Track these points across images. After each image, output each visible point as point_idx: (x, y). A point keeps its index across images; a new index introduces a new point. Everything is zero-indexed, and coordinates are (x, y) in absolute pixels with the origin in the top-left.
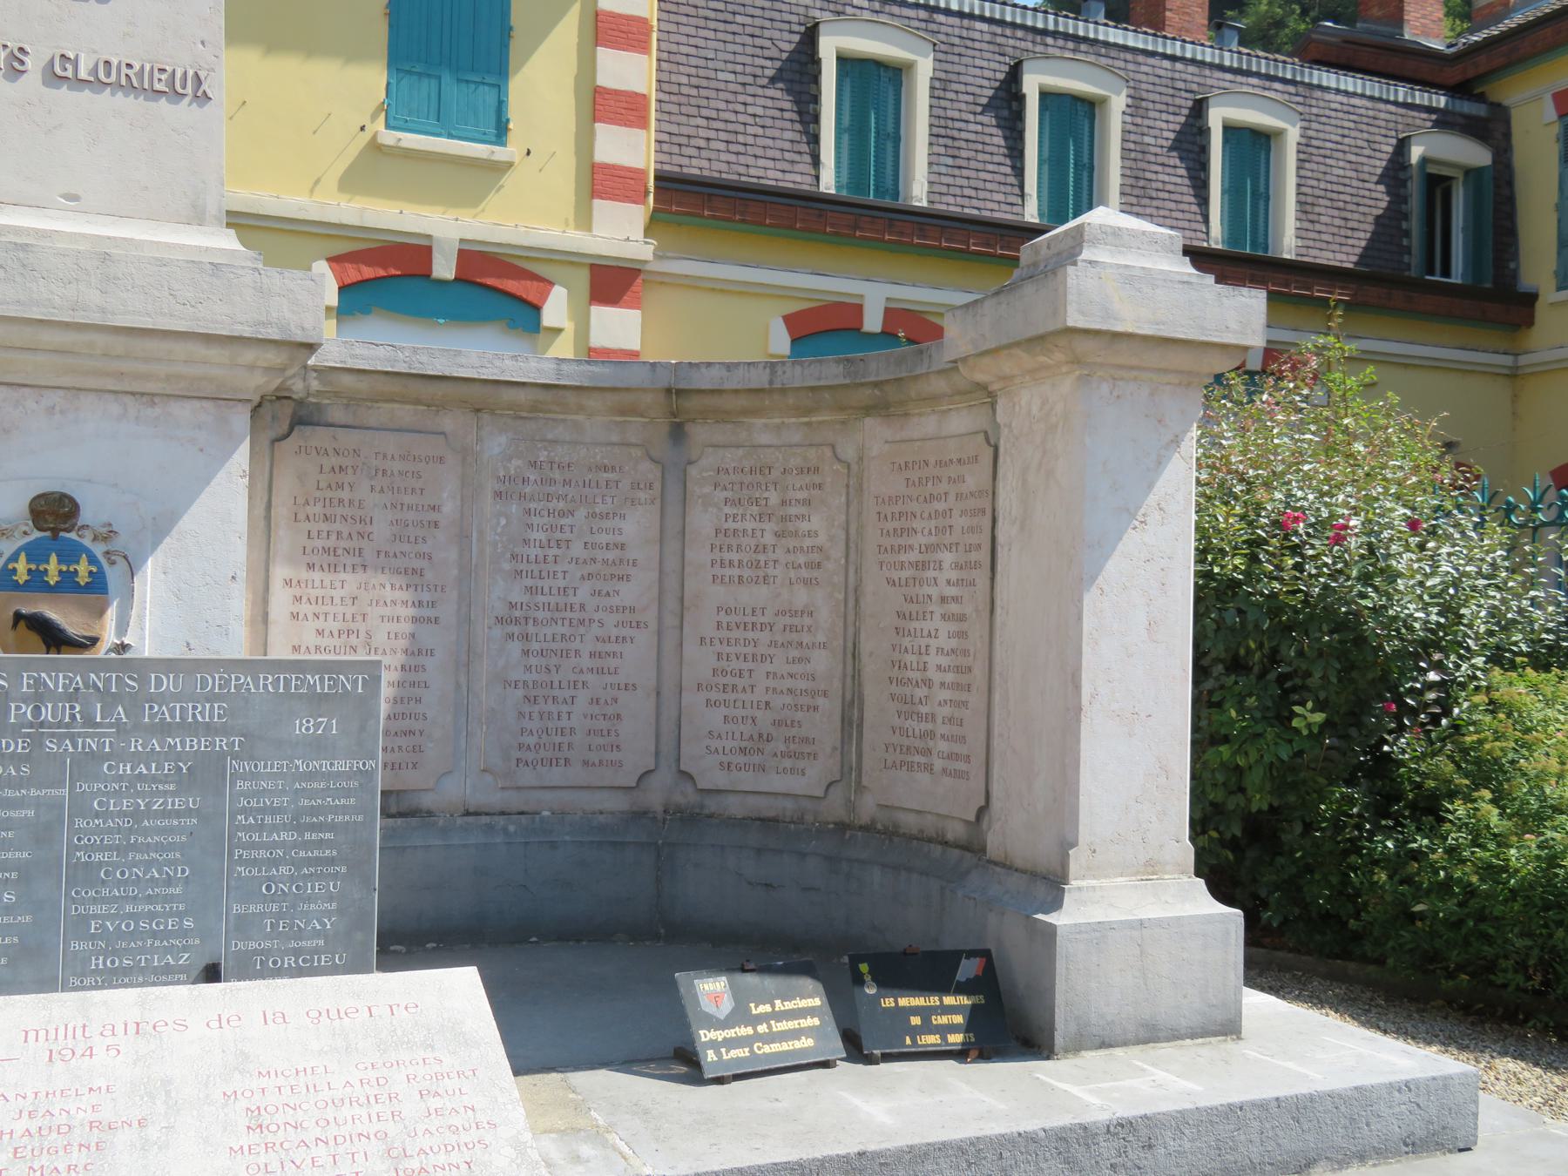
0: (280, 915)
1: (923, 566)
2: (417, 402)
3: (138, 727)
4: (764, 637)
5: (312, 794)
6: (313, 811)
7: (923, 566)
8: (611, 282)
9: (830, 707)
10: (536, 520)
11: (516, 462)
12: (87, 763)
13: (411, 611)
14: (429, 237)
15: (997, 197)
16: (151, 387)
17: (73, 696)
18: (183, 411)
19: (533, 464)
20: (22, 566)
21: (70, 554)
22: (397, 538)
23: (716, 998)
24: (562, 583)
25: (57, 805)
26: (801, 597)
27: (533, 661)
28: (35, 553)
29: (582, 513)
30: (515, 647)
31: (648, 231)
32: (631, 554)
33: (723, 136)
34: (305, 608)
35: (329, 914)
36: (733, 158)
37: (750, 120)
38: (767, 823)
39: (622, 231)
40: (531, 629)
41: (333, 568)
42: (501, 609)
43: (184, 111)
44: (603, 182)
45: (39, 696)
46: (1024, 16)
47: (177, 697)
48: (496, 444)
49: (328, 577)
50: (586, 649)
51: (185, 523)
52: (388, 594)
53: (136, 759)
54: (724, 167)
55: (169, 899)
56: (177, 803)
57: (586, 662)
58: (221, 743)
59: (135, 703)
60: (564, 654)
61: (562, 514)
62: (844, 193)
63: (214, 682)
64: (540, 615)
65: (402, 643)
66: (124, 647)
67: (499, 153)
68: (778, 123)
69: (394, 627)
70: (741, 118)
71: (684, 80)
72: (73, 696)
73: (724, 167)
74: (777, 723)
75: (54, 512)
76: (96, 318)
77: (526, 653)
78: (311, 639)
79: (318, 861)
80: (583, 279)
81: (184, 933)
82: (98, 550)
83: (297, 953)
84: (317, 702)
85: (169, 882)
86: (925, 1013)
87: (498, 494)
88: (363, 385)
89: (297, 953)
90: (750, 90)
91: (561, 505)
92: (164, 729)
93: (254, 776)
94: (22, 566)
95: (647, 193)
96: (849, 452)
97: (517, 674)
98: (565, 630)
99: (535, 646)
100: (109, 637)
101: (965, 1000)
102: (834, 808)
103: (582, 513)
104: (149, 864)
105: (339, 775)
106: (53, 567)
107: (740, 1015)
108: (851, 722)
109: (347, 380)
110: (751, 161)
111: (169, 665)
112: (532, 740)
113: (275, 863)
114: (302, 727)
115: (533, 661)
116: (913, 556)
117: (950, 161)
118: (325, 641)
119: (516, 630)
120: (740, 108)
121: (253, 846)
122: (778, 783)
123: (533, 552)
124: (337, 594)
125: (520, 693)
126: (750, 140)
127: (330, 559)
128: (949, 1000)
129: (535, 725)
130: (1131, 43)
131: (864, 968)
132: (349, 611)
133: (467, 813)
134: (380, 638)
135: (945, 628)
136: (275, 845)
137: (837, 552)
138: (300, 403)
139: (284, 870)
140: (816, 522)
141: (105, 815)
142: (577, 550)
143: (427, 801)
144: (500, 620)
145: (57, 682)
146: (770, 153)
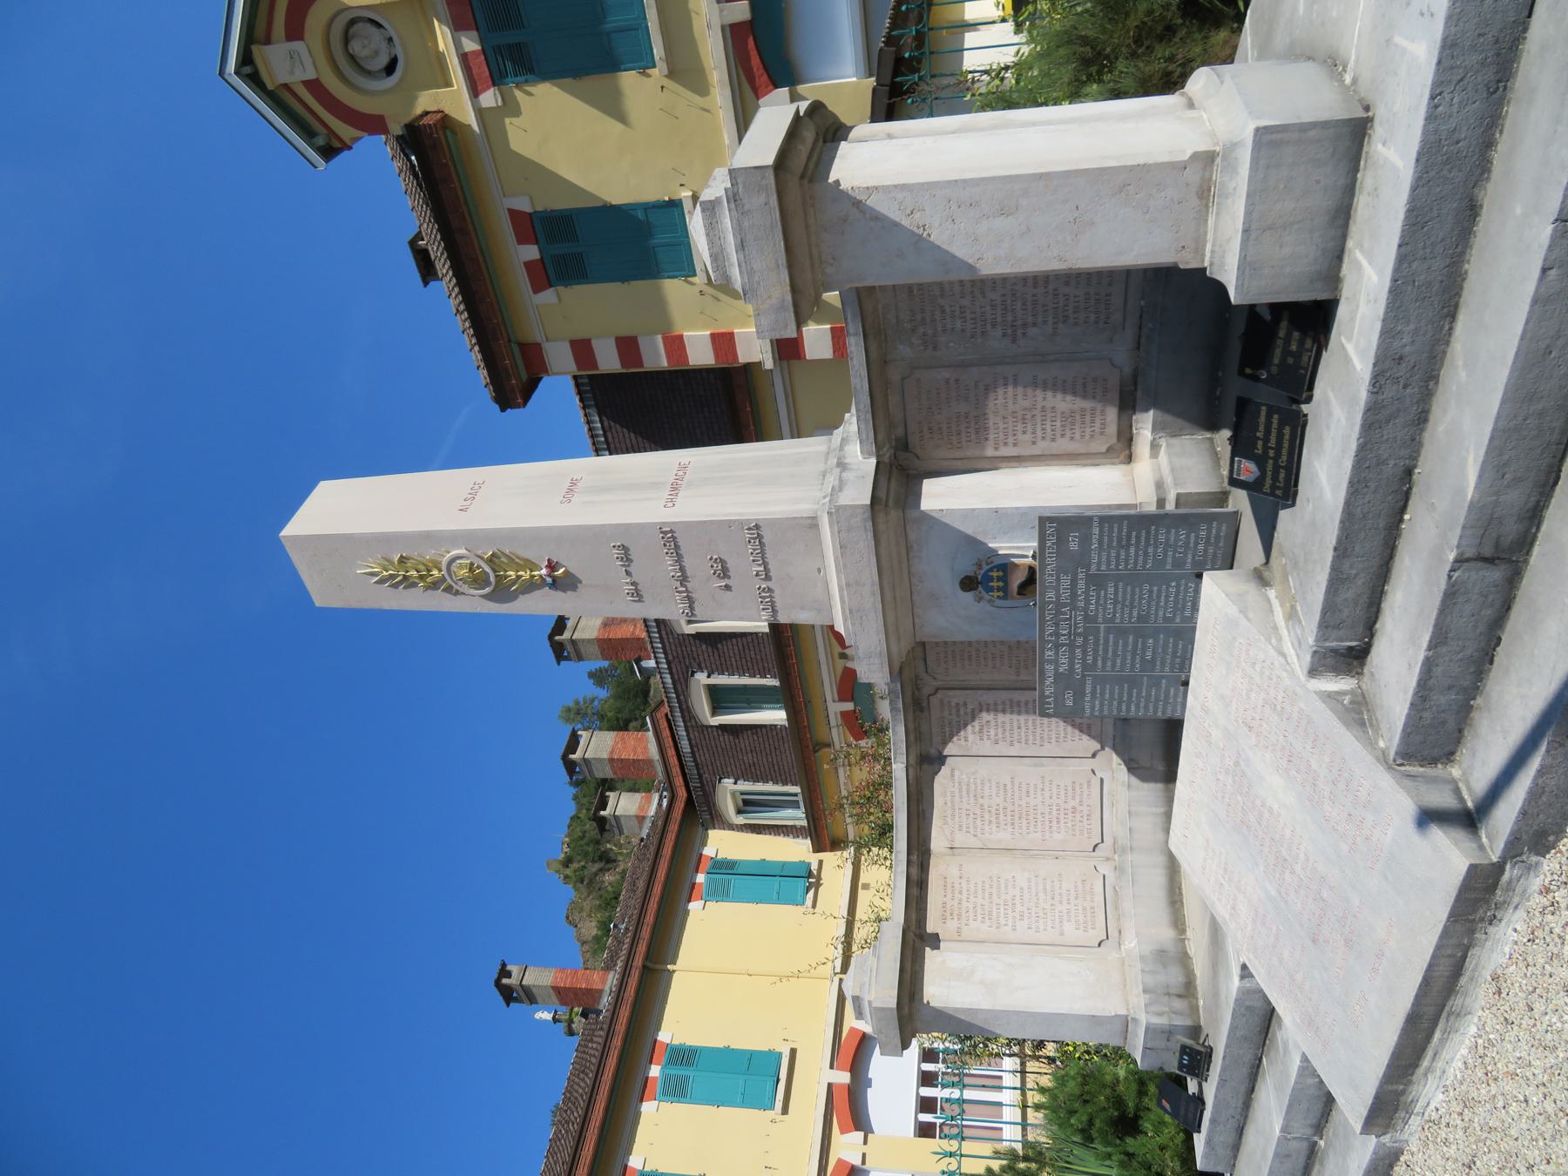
0: (1175, 551)
2: (886, 396)
5: (1111, 541)
6: (1120, 540)
10: (949, 327)
11: (914, 340)
13: (1010, 389)
16: (904, 551)
17: (1057, 625)
18: (912, 536)
19: (913, 330)
20: (996, 594)
24: (988, 308)
25: (1108, 630)
27: (1040, 319)
29: (941, 301)
30: (1032, 331)
34: (1011, 440)
35: (1177, 533)
40: (1019, 323)
41: (986, 429)
43: (765, 533)
47: (1058, 591)
48: (904, 351)
49: (992, 431)
51: (970, 532)
52: (1000, 401)
55: (1159, 591)
56: (1111, 590)
58: (1081, 576)
61: (943, 312)
64: (1010, 318)
65: (1029, 391)
66: (1034, 557)
69: (1020, 397)
72: (1057, 625)
75: (968, 584)
76: (877, 588)
77: (1035, 325)
79: (1147, 539)
81: (1178, 586)
82: (986, 568)
83: (1197, 544)
84: (1061, 541)
85: (1151, 591)
86: (1286, 352)
87: (935, 348)
89: (1197, 544)
91: (938, 313)
92: (1074, 596)
93: (1099, 564)
98: (1019, 305)
99: (1030, 319)
101: (1284, 324)
103: (941, 301)
104: (1141, 598)
105: (1101, 532)
109: (880, 437)
112: (1092, 317)
113: (1146, 554)
114: (1074, 546)
115: (1040, 319)
118: (1029, 429)
119: (1019, 332)
121: (1136, 563)
124: (1001, 426)
125: (1060, 326)
127: (980, 430)
128: (1282, 334)
131: (1248, 371)
132: (1011, 419)
133: (1138, 348)
134: (1027, 404)
136: (1137, 555)
138: (896, 448)
139: (1151, 550)
141: (1114, 613)
143: (1128, 370)
144: (1014, 341)
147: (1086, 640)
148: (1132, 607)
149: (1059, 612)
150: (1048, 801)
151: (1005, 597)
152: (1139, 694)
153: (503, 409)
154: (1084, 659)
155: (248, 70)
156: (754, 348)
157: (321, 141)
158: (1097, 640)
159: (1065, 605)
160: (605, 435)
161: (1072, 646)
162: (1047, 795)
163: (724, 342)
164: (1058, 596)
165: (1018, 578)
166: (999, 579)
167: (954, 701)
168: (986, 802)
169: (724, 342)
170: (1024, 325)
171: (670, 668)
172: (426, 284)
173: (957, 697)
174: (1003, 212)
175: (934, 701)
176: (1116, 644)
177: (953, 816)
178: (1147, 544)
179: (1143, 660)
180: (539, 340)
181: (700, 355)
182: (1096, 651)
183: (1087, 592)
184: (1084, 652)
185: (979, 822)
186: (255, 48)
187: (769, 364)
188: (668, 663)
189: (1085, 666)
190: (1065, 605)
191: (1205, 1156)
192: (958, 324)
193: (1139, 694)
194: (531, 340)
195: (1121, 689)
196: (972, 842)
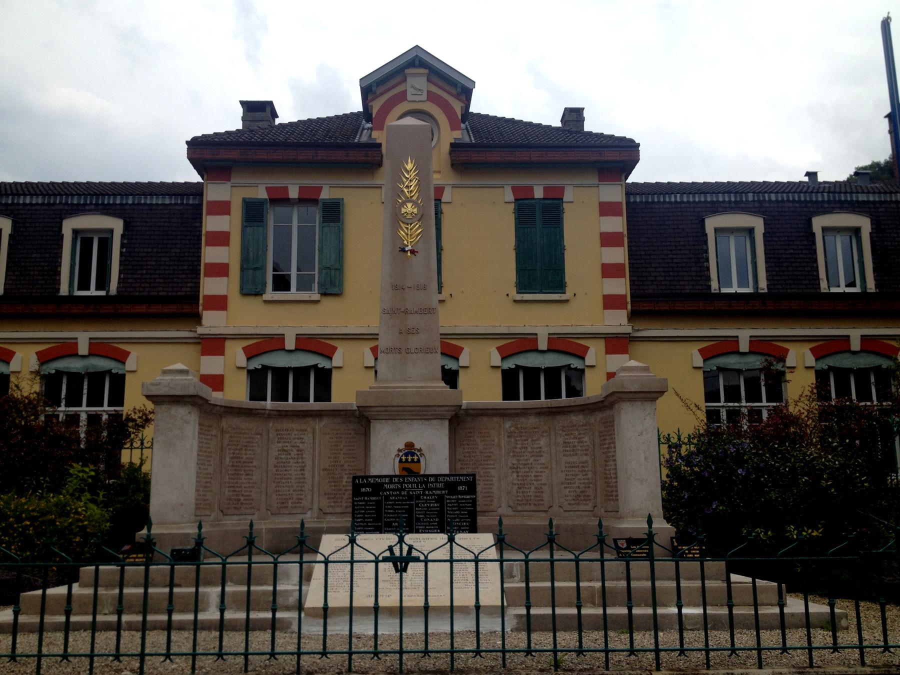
1: (608, 448)
3: (427, 489)
4: (577, 469)
7: (608, 448)
8: (617, 343)
12: (418, 497)
14: (536, 334)
18: (435, 422)
20: (404, 458)
21: (413, 454)
26: (584, 458)
28: (406, 455)
30: (515, 475)
33: (663, 274)
36: (668, 283)
37: (675, 265)
39: (618, 321)
42: (510, 465)
44: (611, 302)
50: (533, 474)
57: (533, 478)
59: (426, 483)
60: (527, 476)
63: (441, 479)
67: (564, 297)
70: (671, 265)
71: (643, 253)
74: (581, 492)
75: (409, 445)
80: (601, 344)
88: (475, 412)
90: (674, 252)
92: (431, 489)
94: (404, 458)
95: (627, 304)
97: (516, 482)
106: (410, 458)
117: (777, 269)
120: (670, 261)
123: (518, 450)
126: (676, 274)
140: (586, 439)
146: (685, 278)
148: (425, 514)
151: (401, 461)
153: (187, 142)
154: (393, 495)
155: (417, 63)
156: (213, 322)
159: (426, 486)
160: (145, 204)
162: (247, 485)
164: (432, 483)
165: (413, 467)
166: (413, 460)
168: (244, 452)
170: (517, 472)
172: (243, 103)
174: (646, 458)
175: (304, 427)
177: (237, 433)
180: (233, 181)
182: (399, 500)
183: (434, 495)
185: (233, 447)
186: (427, 71)
187: (200, 330)
190: (426, 486)
192: (519, 446)
196: (226, 442)
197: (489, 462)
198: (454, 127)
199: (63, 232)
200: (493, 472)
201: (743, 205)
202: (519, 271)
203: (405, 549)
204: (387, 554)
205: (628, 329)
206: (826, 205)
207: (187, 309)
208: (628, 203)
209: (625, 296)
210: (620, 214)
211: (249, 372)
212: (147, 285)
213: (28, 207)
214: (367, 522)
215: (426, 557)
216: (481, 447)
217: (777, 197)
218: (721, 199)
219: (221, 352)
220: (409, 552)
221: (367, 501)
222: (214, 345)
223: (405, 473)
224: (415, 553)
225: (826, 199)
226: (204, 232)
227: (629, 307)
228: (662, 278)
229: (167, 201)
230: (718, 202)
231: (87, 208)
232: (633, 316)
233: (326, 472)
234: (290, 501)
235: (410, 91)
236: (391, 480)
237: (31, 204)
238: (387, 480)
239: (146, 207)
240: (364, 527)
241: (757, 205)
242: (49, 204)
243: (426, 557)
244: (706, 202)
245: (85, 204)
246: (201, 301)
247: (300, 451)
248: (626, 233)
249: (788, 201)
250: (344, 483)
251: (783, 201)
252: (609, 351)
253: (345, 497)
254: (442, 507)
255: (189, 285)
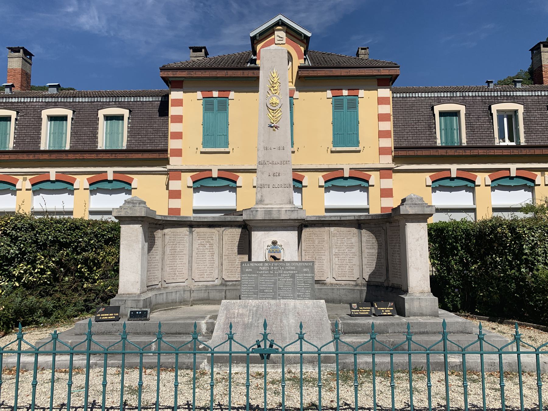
1: (395, 246)
3: (285, 270)
7: (395, 246)
8: (386, 172)
9: (384, 267)
15: (486, 140)
17: (278, 266)
21: (277, 248)
22: (319, 243)
23: (355, 306)
28: (272, 248)
30: (337, 259)
31: (393, 161)
32: (353, 244)
33: (411, 136)
38: (377, 286)
39: (387, 161)
42: (334, 253)
44: (383, 151)
45: (274, 266)
46: (491, 94)
53: (285, 274)
54: (412, 143)
57: (348, 261)
62: (444, 145)
63: (294, 264)
67: (358, 149)
68: (425, 131)
72: (278, 266)
73: (412, 143)
78: (307, 258)
84: (306, 267)
92: (288, 270)
96: (385, 228)
97: (337, 263)
100: (282, 259)
102: (386, 284)
107: (358, 309)
108: (387, 270)
110: (418, 140)
111: (288, 262)
114: (305, 270)
116: (393, 244)
117: (472, 133)
122: (378, 280)
123: (339, 244)
129: (340, 271)
130: (524, 95)
135: (398, 255)
137: (384, 244)
142: (345, 244)
145: (276, 264)
146: (423, 138)
147: (272, 274)
148: (284, 285)
149: (282, 267)
150: (178, 265)
151: (270, 252)
152: (251, 289)
154: (265, 274)
155: (280, 24)
156: (175, 163)
157: (258, 38)
158: (270, 277)
159: (284, 268)
161: (270, 270)
162: (180, 265)
163: (178, 153)
165: (277, 255)
167: (214, 236)
168: (178, 246)
169: (178, 153)
171: (21, 102)
173: (216, 237)
176: (270, 282)
177: (174, 235)
178: (305, 288)
179: (264, 289)
181: (173, 144)
184: (267, 274)
187: (169, 167)
188: (24, 102)
189: (263, 274)
190: (284, 268)
191: (80, 324)
193: (251, 289)
194: (184, 85)
195: (252, 284)
196: (167, 241)
197: (321, 251)
198: (299, 58)
199: (99, 116)
200: (323, 257)
201: (454, 99)
202: (334, 134)
203: (268, 344)
204: (256, 347)
205: (393, 166)
206: (499, 98)
207: (162, 156)
208: (393, 97)
209: (391, 148)
210: (389, 104)
211: (194, 188)
212: (142, 144)
213: (81, 104)
214: (249, 289)
215: (283, 350)
216: (317, 242)
217: (472, 94)
218: (442, 95)
219: (179, 178)
220: (271, 346)
221: (249, 277)
222: (175, 174)
223: (273, 260)
224: (275, 347)
225: (499, 95)
226: (170, 116)
227: (393, 154)
228: (411, 138)
229: (151, 100)
230: (441, 97)
231: (111, 103)
232: (396, 159)
233: (226, 257)
234: (205, 274)
235: (277, 38)
236: (264, 265)
237: (82, 102)
238: (261, 264)
239: (140, 103)
240: (248, 292)
241: (462, 98)
242: (91, 102)
243: (283, 350)
244: (434, 97)
245: (110, 102)
246: (169, 152)
247: (211, 245)
248: (392, 114)
249: (479, 96)
250: (237, 263)
251: (476, 96)
252: (381, 177)
253: (237, 274)
254: (294, 282)
255: (163, 143)
